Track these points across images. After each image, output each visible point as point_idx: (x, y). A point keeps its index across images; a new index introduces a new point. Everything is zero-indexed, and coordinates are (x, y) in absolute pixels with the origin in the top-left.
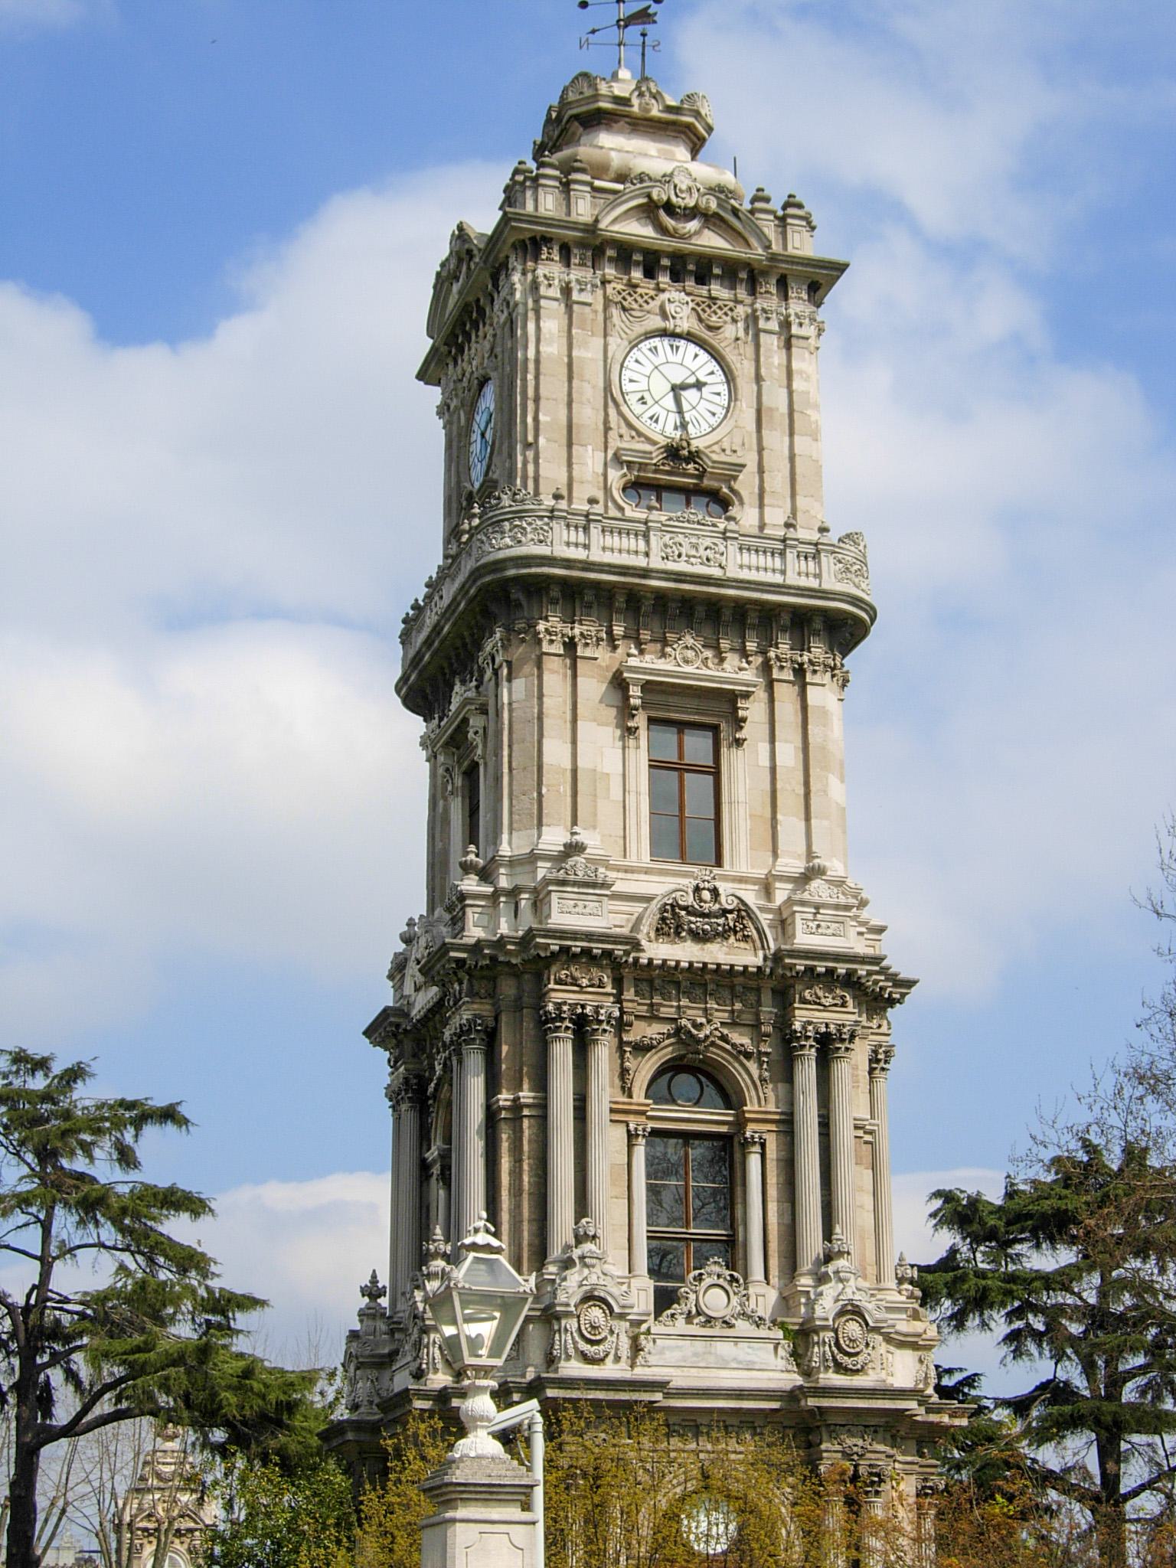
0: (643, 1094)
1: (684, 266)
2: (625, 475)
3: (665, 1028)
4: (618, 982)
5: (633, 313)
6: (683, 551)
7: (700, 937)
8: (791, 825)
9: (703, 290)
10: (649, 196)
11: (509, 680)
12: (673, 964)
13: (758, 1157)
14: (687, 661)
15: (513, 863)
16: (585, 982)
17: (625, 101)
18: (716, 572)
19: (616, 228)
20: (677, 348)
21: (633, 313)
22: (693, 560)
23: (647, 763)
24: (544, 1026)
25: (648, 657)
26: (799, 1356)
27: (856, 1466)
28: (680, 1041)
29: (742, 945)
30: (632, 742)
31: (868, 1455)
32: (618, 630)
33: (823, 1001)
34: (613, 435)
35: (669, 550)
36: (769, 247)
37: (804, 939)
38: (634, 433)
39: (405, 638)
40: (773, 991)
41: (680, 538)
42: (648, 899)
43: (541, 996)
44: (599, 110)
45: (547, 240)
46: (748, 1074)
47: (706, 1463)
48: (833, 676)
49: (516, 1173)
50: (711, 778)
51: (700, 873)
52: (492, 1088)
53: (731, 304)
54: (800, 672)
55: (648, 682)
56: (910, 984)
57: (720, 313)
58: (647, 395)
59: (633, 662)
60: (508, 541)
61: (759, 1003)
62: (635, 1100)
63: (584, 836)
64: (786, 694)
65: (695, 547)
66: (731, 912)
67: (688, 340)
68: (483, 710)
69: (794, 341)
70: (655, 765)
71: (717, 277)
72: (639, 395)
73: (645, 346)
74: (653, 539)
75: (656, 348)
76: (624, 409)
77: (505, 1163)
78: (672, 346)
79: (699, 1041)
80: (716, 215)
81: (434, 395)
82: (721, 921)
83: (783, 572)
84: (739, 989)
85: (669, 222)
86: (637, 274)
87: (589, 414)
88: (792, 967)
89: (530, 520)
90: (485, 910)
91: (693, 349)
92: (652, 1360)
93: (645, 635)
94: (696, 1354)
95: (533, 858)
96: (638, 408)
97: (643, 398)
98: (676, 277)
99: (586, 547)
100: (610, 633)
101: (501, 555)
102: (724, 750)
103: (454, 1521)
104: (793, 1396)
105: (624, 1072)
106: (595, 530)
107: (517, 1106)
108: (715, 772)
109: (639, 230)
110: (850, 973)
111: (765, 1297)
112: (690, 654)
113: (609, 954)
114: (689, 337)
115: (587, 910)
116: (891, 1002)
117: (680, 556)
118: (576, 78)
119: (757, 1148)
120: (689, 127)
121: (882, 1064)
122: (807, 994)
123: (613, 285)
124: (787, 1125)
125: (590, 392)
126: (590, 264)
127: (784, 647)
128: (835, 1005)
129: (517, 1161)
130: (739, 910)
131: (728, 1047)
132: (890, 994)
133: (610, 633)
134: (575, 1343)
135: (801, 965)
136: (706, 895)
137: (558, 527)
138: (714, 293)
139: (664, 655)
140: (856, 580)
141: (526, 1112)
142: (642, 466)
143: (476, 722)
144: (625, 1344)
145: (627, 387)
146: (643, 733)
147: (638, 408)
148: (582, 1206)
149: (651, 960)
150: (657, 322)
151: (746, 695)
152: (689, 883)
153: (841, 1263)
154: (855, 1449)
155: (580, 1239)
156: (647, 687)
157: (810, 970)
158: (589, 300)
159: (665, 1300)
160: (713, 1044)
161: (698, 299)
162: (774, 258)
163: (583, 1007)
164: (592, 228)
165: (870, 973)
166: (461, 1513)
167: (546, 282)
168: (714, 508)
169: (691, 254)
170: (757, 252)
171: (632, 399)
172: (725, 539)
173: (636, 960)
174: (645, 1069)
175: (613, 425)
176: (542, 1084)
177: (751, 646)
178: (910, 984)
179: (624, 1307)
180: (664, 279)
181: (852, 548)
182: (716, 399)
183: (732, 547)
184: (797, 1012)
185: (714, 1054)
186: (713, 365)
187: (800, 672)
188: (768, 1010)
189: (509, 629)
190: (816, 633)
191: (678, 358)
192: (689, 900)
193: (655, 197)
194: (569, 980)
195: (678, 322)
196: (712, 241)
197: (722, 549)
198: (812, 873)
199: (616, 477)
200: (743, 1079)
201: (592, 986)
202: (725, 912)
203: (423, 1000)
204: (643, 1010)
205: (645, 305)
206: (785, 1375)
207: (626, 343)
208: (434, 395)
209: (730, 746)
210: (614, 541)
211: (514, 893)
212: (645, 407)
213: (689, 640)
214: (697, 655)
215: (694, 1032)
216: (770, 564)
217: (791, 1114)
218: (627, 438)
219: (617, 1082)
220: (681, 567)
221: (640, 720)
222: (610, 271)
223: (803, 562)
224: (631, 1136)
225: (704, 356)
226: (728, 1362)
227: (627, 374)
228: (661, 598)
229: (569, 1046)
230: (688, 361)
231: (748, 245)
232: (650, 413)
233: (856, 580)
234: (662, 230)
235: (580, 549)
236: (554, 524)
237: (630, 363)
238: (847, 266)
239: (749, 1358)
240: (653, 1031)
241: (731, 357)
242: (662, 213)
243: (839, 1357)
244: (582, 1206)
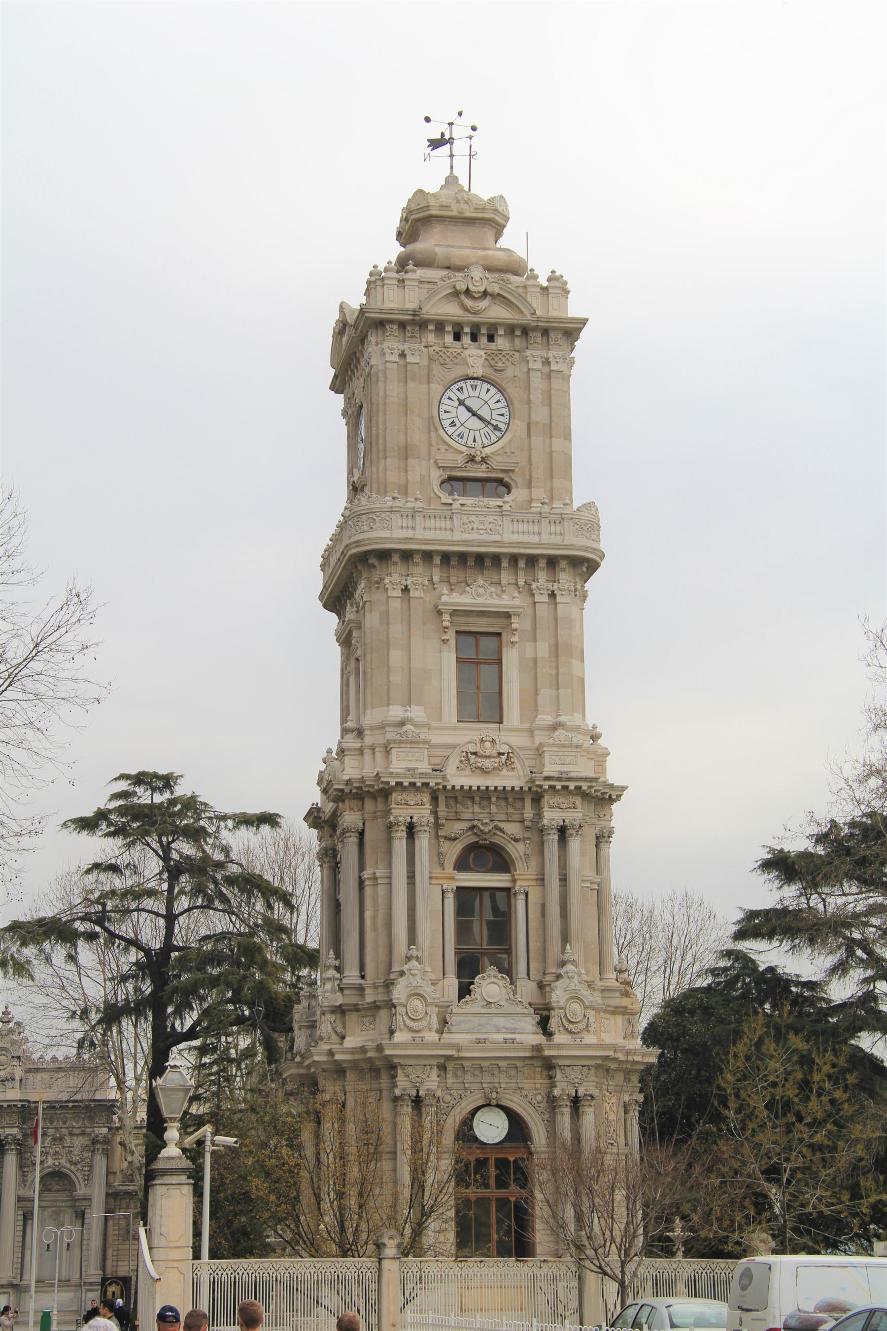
0: (452, 867)
1: (479, 330)
2: (441, 476)
3: (464, 825)
4: (435, 799)
5: (447, 366)
6: (475, 526)
7: (484, 771)
8: (545, 693)
9: (492, 346)
10: (454, 287)
11: (371, 612)
12: (467, 788)
13: (524, 902)
14: (479, 595)
15: (372, 729)
16: (412, 803)
17: (447, 207)
18: (497, 538)
19: (432, 311)
20: (476, 386)
21: (447, 366)
22: (481, 532)
24: (390, 827)
25: (455, 595)
26: (544, 1024)
27: (576, 1091)
28: (475, 834)
29: (510, 773)
30: (445, 647)
31: (585, 1084)
32: (436, 579)
33: (562, 806)
34: (434, 449)
35: (466, 527)
36: (534, 313)
37: (550, 769)
38: (446, 447)
39: (323, 567)
40: (532, 800)
41: (473, 518)
42: (453, 747)
43: (388, 812)
44: (431, 216)
45: (390, 322)
46: (516, 851)
47: (487, 1090)
48: (576, 595)
49: (374, 918)
50: (496, 667)
51: (488, 730)
52: (362, 867)
53: (511, 353)
54: (553, 595)
55: (454, 610)
56: (623, 788)
57: (504, 359)
58: (456, 420)
59: (444, 599)
60: (366, 528)
61: (523, 807)
62: (447, 871)
63: (416, 713)
64: (543, 611)
65: (482, 522)
66: (503, 754)
67: (483, 381)
68: (360, 628)
69: (552, 374)
70: (459, 660)
71: (501, 336)
72: (451, 420)
73: (454, 388)
74: (455, 519)
75: (462, 388)
76: (442, 432)
77: (368, 915)
78: (472, 386)
79: (485, 833)
80: (499, 295)
81: (339, 400)
82: (497, 760)
83: (539, 534)
84: (511, 800)
85: (468, 303)
86: (449, 339)
87: (418, 437)
88: (541, 786)
89: (378, 514)
90: (357, 757)
91: (486, 386)
92: (453, 1029)
93: (453, 580)
94: (480, 1025)
95: (383, 727)
96: (450, 430)
97: (453, 422)
98: (474, 338)
99: (413, 528)
100: (431, 580)
101: (360, 537)
102: (504, 649)
103: (156, 1185)
104: (538, 1048)
105: (440, 854)
106: (419, 518)
107: (375, 878)
108: (499, 662)
109: (451, 311)
110: (578, 788)
111: (527, 989)
112: (481, 590)
113: (426, 785)
115: (414, 759)
116: (611, 800)
117: (473, 529)
118: (416, 193)
119: (523, 897)
120: (489, 220)
121: (606, 839)
122: (551, 802)
123: (434, 348)
124: (541, 880)
125: (417, 422)
126: (418, 336)
128: (569, 808)
129: (376, 911)
130: (508, 753)
131: (504, 836)
132: (610, 796)
133: (431, 580)
134: (404, 1021)
135: (546, 785)
136: (488, 744)
137: (396, 517)
138: (500, 348)
139: (464, 592)
140: (588, 535)
141: (380, 881)
142: (452, 468)
143: (355, 634)
144: (435, 1020)
145: (444, 416)
146: (453, 643)
147: (450, 430)
148: (412, 939)
149: (453, 787)
150: (459, 371)
151: (517, 614)
152: (477, 738)
153: (569, 967)
154: (576, 1080)
155: (408, 959)
156: (454, 613)
157: (552, 787)
158: (418, 361)
159: (464, 991)
160: (495, 834)
161: (489, 352)
162: (539, 319)
163: (411, 818)
164: (415, 313)
165: (589, 787)
166: (157, 1182)
167: (389, 351)
168: (502, 489)
169: (484, 323)
170: (527, 319)
171: (446, 423)
172: (502, 515)
173: (444, 787)
174: (453, 851)
175: (434, 443)
176: (390, 865)
177: (521, 582)
178: (623, 788)
179: (434, 999)
180: (466, 340)
181: (586, 514)
183: (507, 522)
184: (545, 814)
185: (496, 840)
186: (498, 396)
187: (553, 595)
188: (528, 813)
189: (369, 580)
190: (564, 570)
191: (476, 394)
192: (477, 749)
193: (458, 288)
194: (403, 802)
195: (476, 369)
196: (497, 313)
197: (500, 522)
198: (555, 727)
199: (436, 476)
200: (514, 854)
201: (417, 805)
203: (329, 807)
204: (452, 816)
205: (454, 359)
206: (536, 1036)
207: (442, 387)
208: (339, 400)
209: (507, 645)
210: (432, 523)
211: (373, 748)
212: (455, 428)
213: (480, 581)
214: (485, 590)
215: (482, 828)
216: (531, 529)
217: (543, 875)
218: (443, 450)
219: (436, 859)
220: (474, 536)
221: (451, 635)
222: (431, 338)
223: (553, 527)
224: (443, 892)
225: (493, 390)
226: (499, 1029)
227: (443, 407)
228: (463, 557)
229: (404, 841)
230: (483, 395)
231: (521, 312)
232: (458, 432)
233: (588, 535)
234: (466, 309)
235: (410, 531)
236: (393, 515)
237: (445, 400)
238: (587, 320)
239: (512, 1026)
240: (458, 827)
241: (511, 390)
242: (463, 297)
243: (566, 1024)
244: (412, 939)
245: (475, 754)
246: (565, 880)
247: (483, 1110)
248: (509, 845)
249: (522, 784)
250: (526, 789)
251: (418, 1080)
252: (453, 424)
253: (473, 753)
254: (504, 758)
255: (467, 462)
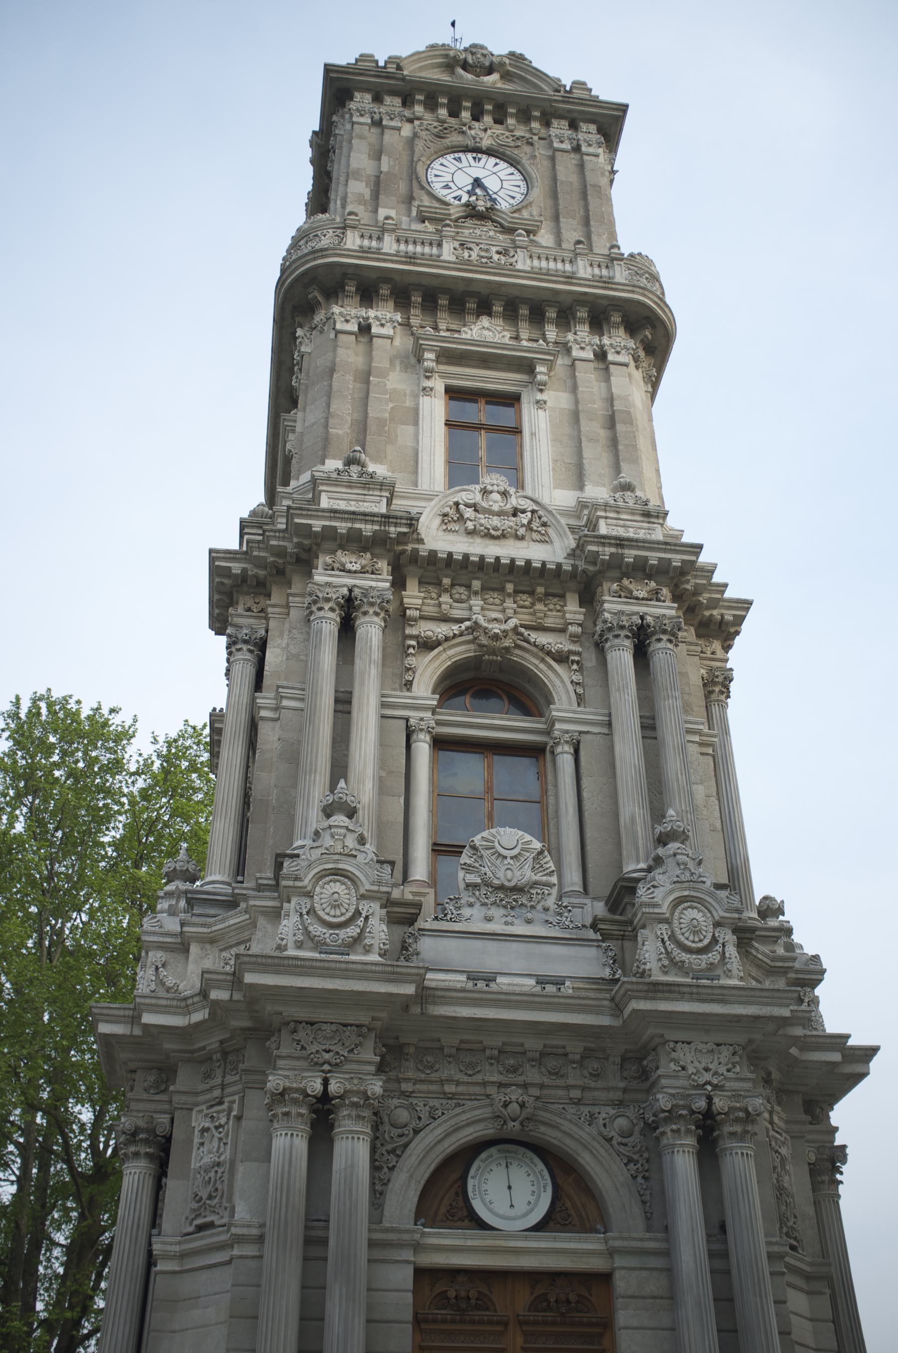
20: (480, 159)
23: (443, 422)
58: (451, 184)
66: (524, 512)
73: (450, 157)
74: (445, 245)
78: (474, 158)
91: (493, 160)
114: (490, 152)
127: (583, 332)
136: (496, 496)
182: (517, 189)
185: (518, 656)
202: (515, 512)
212: (449, 191)
225: (503, 165)
242: (460, 71)
245: (475, 507)
246: (653, 728)
247: (493, 1150)
248: (542, 666)
249: (560, 559)
250: (567, 567)
251: (327, 1056)
252: (447, 187)
253: (467, 505)
254: (524, 519)
255: (466, 217)
